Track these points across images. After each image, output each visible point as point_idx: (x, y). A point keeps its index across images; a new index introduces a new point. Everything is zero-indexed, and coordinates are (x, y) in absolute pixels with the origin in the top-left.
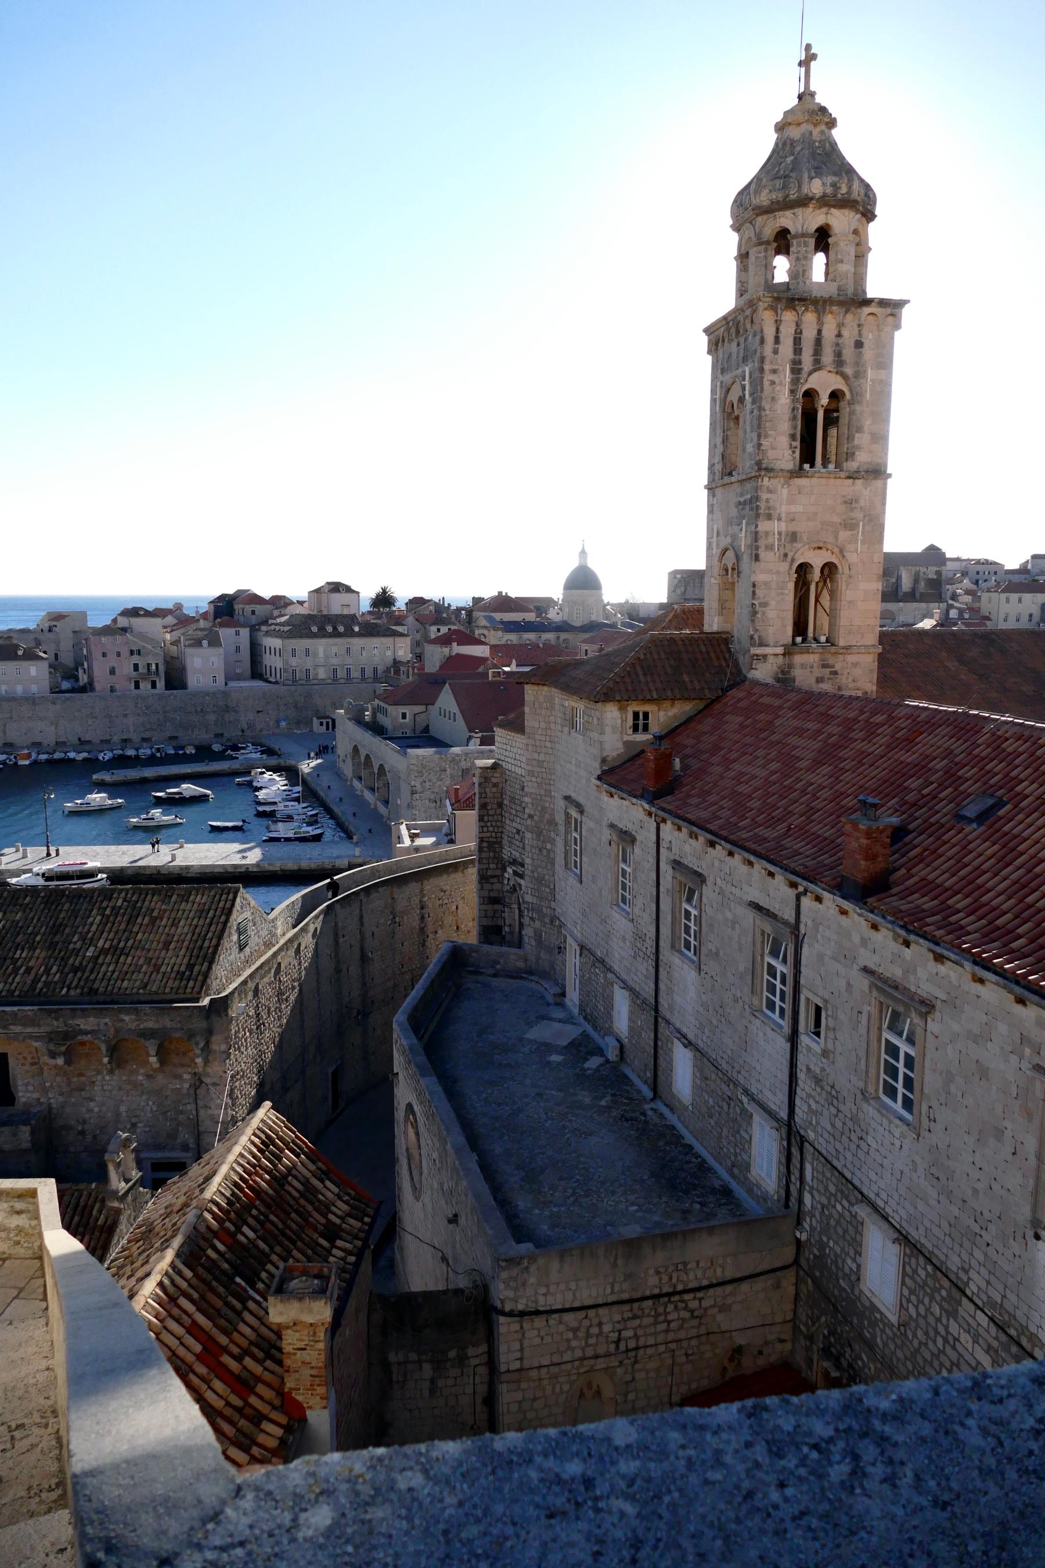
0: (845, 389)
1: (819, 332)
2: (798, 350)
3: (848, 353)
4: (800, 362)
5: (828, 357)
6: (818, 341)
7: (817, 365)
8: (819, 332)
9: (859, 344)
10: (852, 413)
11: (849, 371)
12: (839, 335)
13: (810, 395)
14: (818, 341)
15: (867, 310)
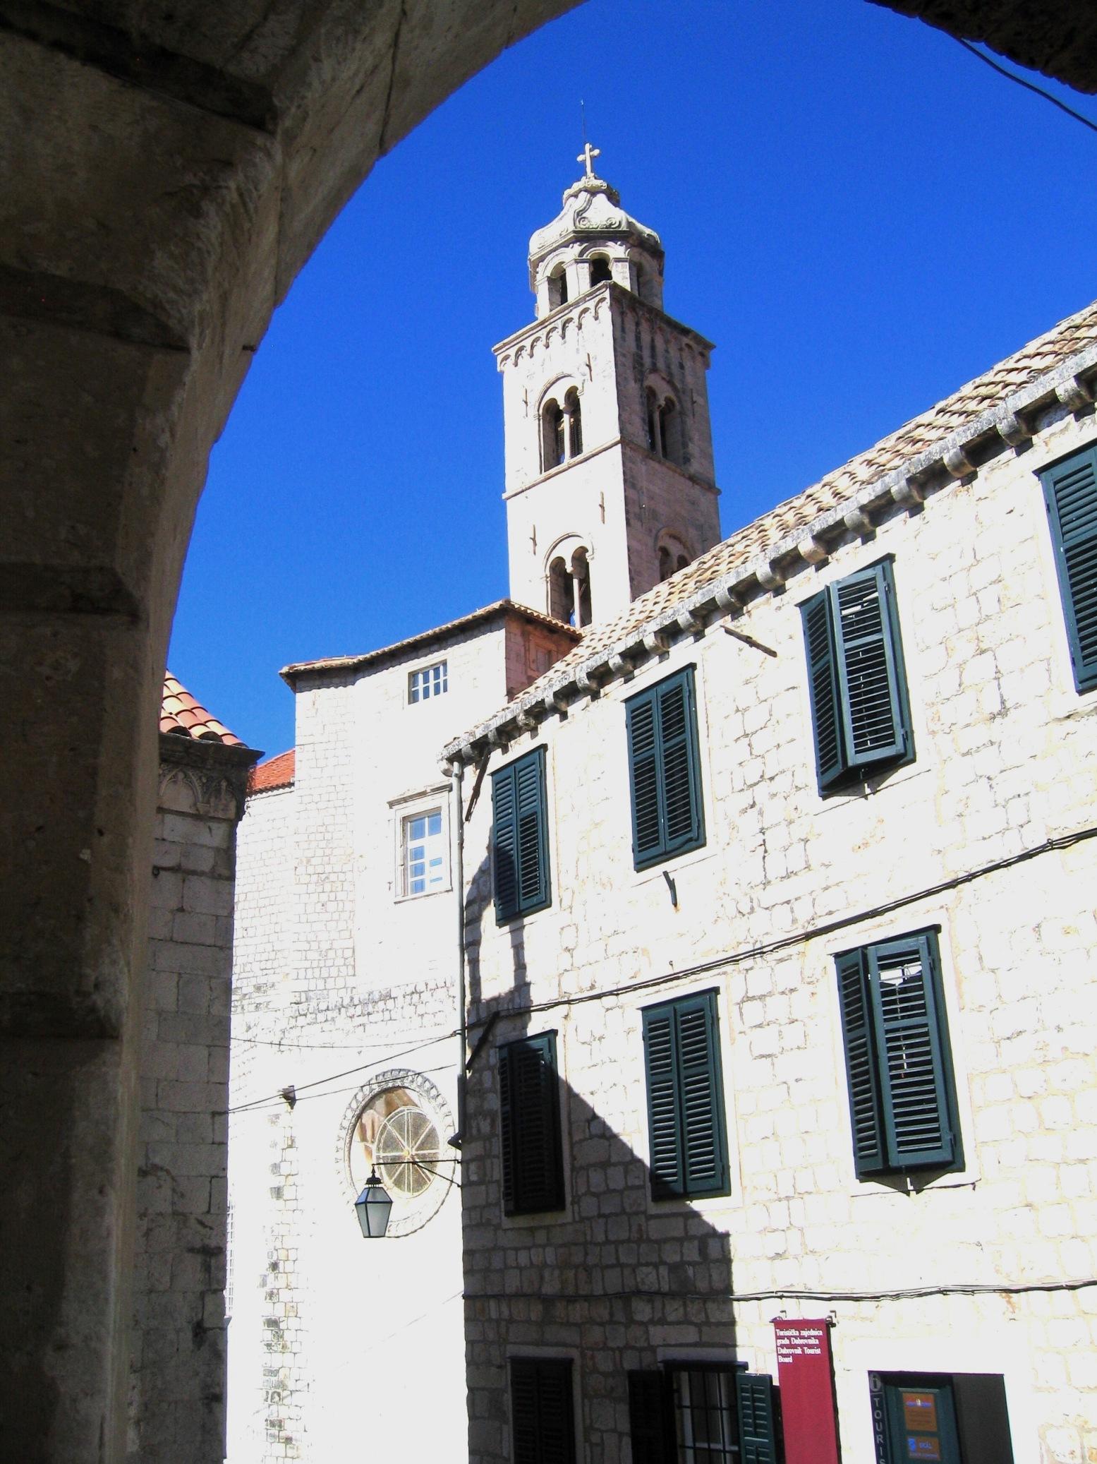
0: (674, 399)
1: (653, 340)
2: (639, 347)
3: (675, 369)
4: (641, 358)
5: (661, 364)
6: (653, 348)
7: (654, 369)
8: (653, 340)
9: (682, 367)
10: (683, 422)
11: (679, 386)
12: (667, 351)
13: (651, 394)
14: (653, 348)
15: (685, 340)
